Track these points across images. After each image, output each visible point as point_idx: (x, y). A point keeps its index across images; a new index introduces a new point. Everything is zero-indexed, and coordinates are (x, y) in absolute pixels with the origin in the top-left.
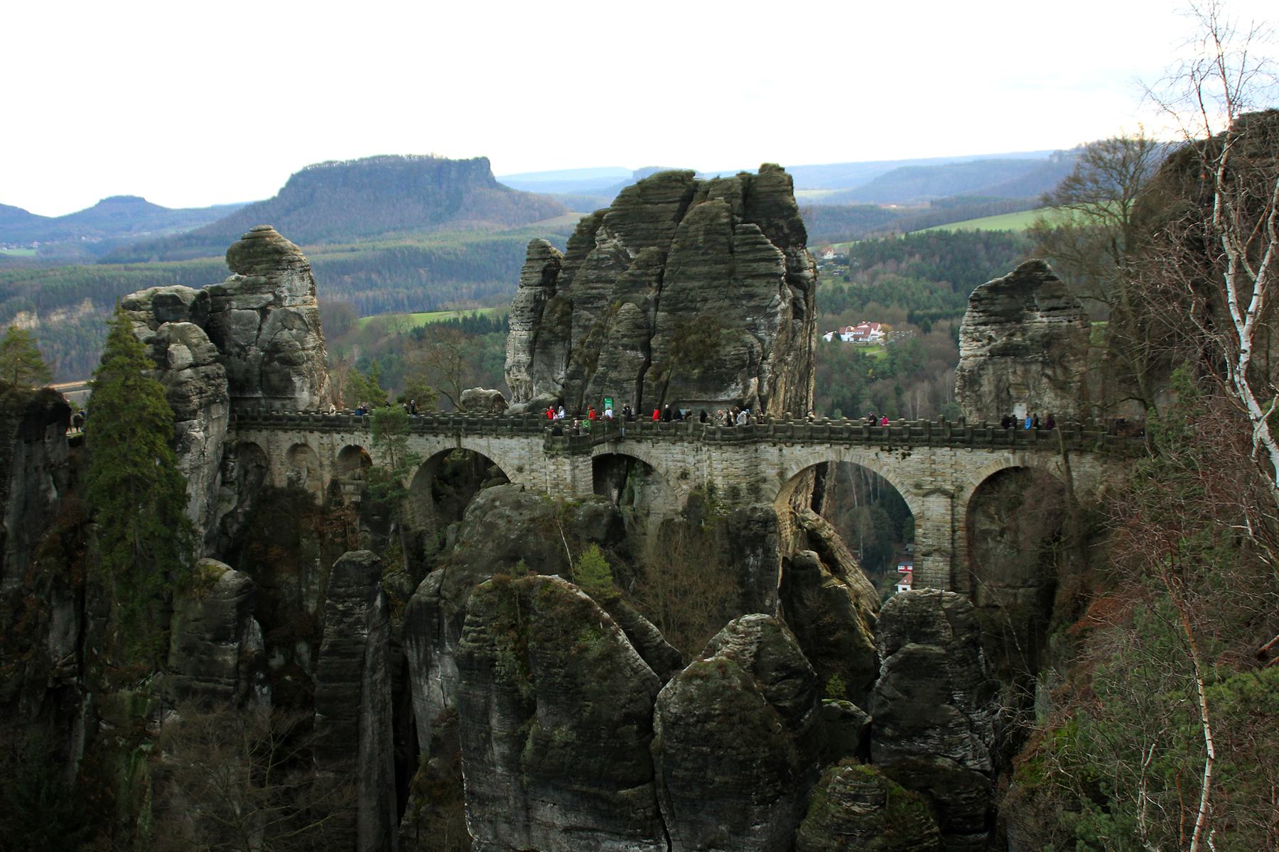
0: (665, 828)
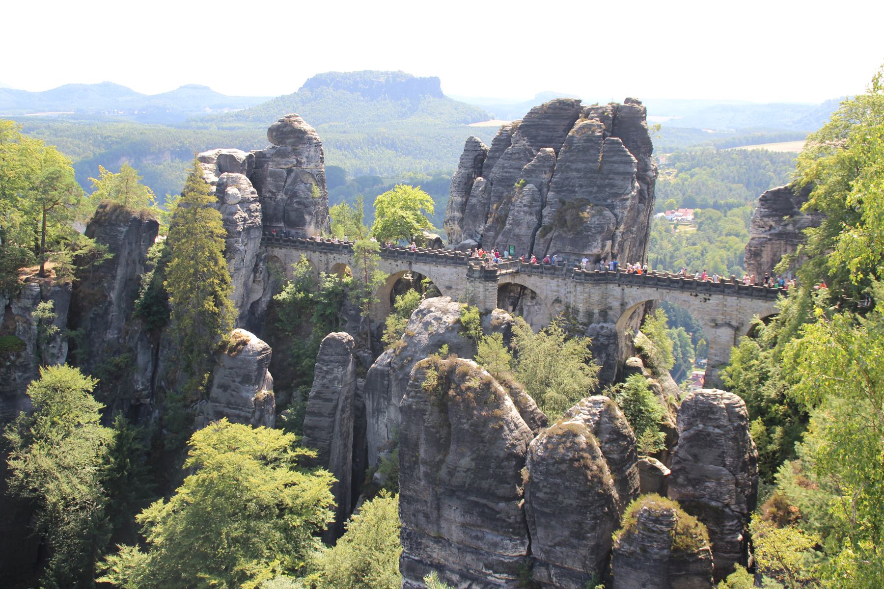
0: (528, 530)
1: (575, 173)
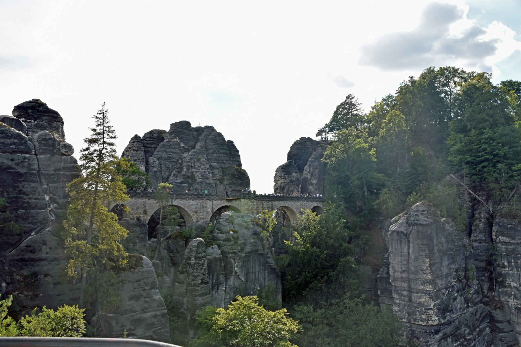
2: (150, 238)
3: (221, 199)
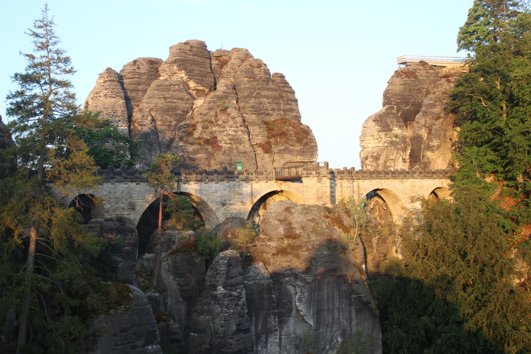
1: (265, 100)
2: (142, 252)
3: (268, 179)
